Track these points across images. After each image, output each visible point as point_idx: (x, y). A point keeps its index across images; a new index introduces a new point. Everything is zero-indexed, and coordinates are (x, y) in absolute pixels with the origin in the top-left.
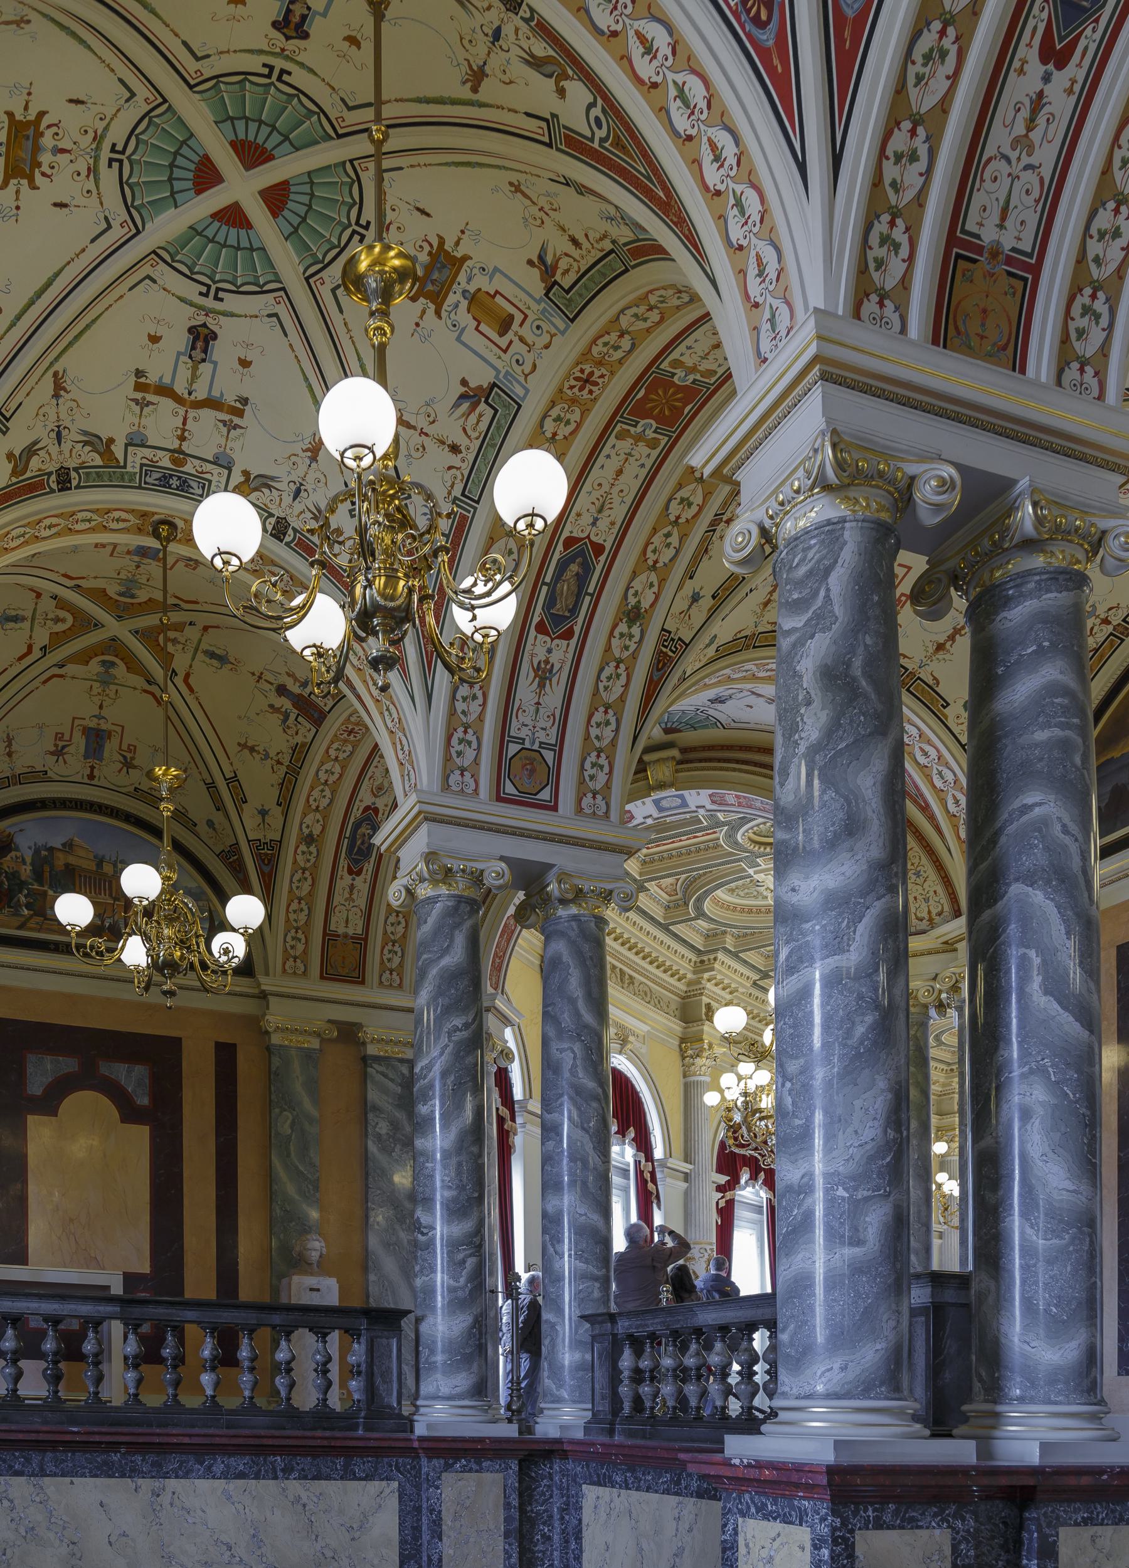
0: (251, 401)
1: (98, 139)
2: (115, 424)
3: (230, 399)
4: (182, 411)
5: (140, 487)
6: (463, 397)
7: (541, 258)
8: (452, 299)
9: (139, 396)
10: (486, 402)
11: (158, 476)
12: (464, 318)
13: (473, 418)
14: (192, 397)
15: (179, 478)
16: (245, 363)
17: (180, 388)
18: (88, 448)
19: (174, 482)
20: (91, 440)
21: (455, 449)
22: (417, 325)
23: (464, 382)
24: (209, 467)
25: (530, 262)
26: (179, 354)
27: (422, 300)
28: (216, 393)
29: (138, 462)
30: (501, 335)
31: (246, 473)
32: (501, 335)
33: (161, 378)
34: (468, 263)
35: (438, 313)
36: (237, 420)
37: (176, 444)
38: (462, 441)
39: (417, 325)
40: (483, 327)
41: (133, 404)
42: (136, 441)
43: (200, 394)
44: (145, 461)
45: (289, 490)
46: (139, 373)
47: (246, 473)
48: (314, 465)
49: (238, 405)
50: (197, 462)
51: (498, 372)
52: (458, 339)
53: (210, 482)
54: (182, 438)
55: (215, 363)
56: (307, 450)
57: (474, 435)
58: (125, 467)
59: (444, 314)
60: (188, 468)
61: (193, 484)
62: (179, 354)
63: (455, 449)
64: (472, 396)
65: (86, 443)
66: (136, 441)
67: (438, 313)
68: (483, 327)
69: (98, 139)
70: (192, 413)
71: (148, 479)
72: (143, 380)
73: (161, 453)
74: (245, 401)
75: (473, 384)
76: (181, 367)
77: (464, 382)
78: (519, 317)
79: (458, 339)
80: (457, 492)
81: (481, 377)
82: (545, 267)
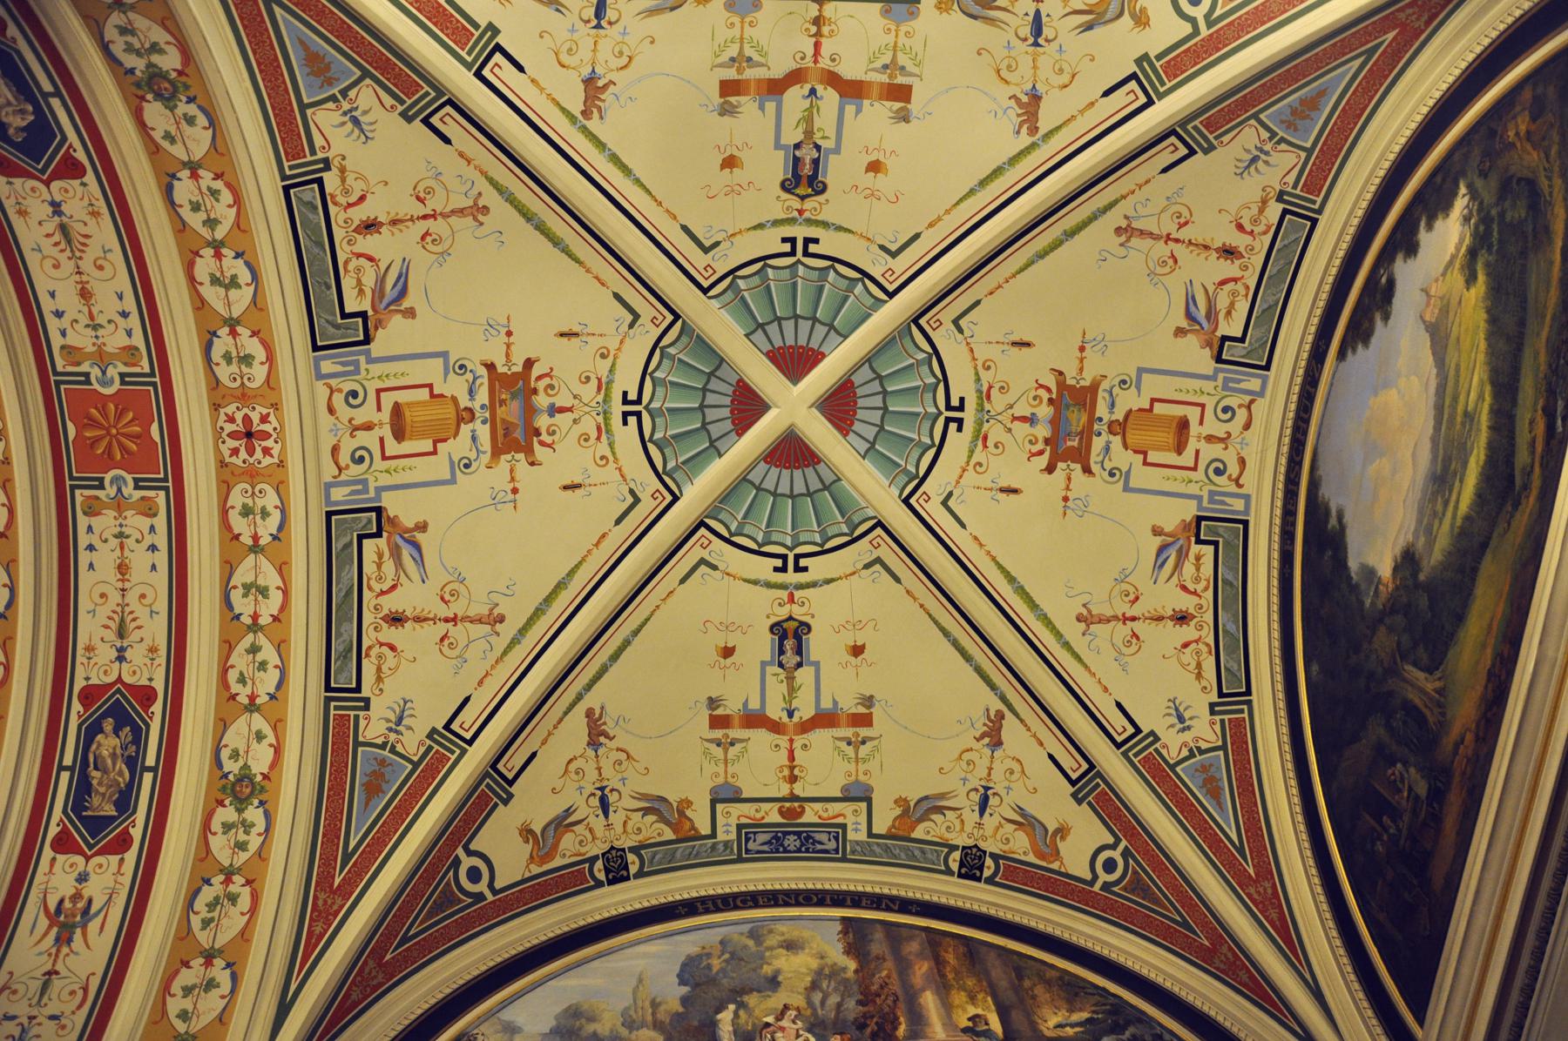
0: (878, 697)
1: (604, 386)
2: (688, 777)
4: (783, 741)
5: (740, 860)
9: (718, 734)
11: (766, 837)
14: (796, 719)
15: (798, 834)
17: (775, 712)
18: (651, 818)
19: (792, 842)
20: (655, 806)
25: (1180, 332)
26: (764, 664)
28: (826, 704)
29: (733, 821)
30: (1180, 449)
33: (746, 704)
34: (1105, 385)
37: (784, 790)
41: (713, 747)
42: (725, 795)
43: (806, 711)
44: (744, 821)
46: (713, 703)
50: (818, 806)
55: (817, 665)
58: (714, 835)
60: (809, 816)
62: (764, 664)
65: (646, 811)
66: (725, 795)
68: (1153, 457)
69: (604, 386)
70: (799, 740)
71: (751, 845)
72: (719, 712)
73: (765, 806)
74: (869, 701)
76: (771, 681)
77: (1157, 531)
78: (1193, 414)
79: (1127, 488)
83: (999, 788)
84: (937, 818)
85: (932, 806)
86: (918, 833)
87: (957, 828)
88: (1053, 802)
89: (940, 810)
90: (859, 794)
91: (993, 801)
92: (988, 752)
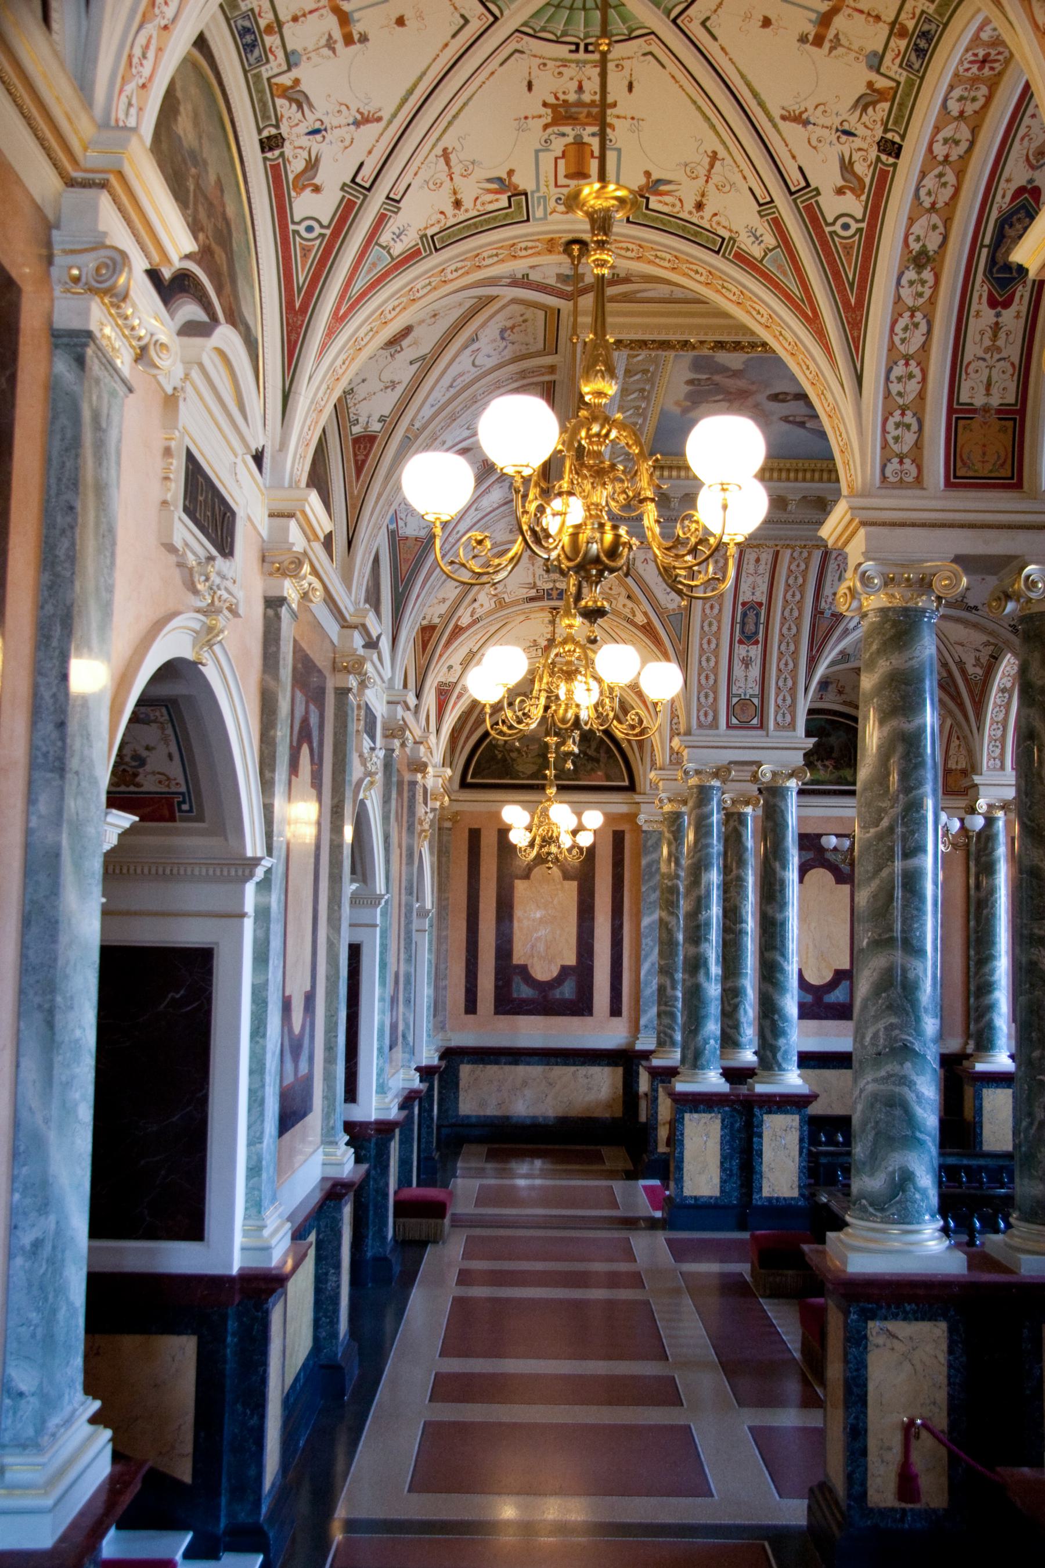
3: (356, 29)
6: (500, 180)
7: (658, 181)
8: (567, 129)
10: (509, 198)
12: (558, 145)
13: (491, 197)
16: (400, 22)
21: (458, 204)
22: (526, 118)
23: (511, 173)
24: (280, 54)
27: (549, 111)
31: (297, 82)
32: (566, 176)
35: (546, 127)
36: (340, 46)
38: (468, 203)
39: (526, 118)
40: (561, 163)
45: (311, 123)
47: (297, 82)
48: (352, 127)
49: (356, 37)
50: (278, 41)
51: (538, 190)
52: (537, 152)
53: (268, 61)
54: (295, 19)
56: (361, 114)
57: (479, 207)
59: (550, 130)
60: (269, 40)
61: (256, 53)
63: (458, 204)
64: (503, 184)
67: (546, 127)
68: (561, 163)
75: (515, 179)
79: (537, 152)
80: (430, 232)
81: (524, 181)
82: (654, 186)
83: (329, 136)
84: (294, 106)
85: (299, 100)
86: (279, 102)
87: (293, 125)
88: (333, 175)
89: (300, 106)
90: (291, 60)
91: (319, 137)
92: (351, 120)
